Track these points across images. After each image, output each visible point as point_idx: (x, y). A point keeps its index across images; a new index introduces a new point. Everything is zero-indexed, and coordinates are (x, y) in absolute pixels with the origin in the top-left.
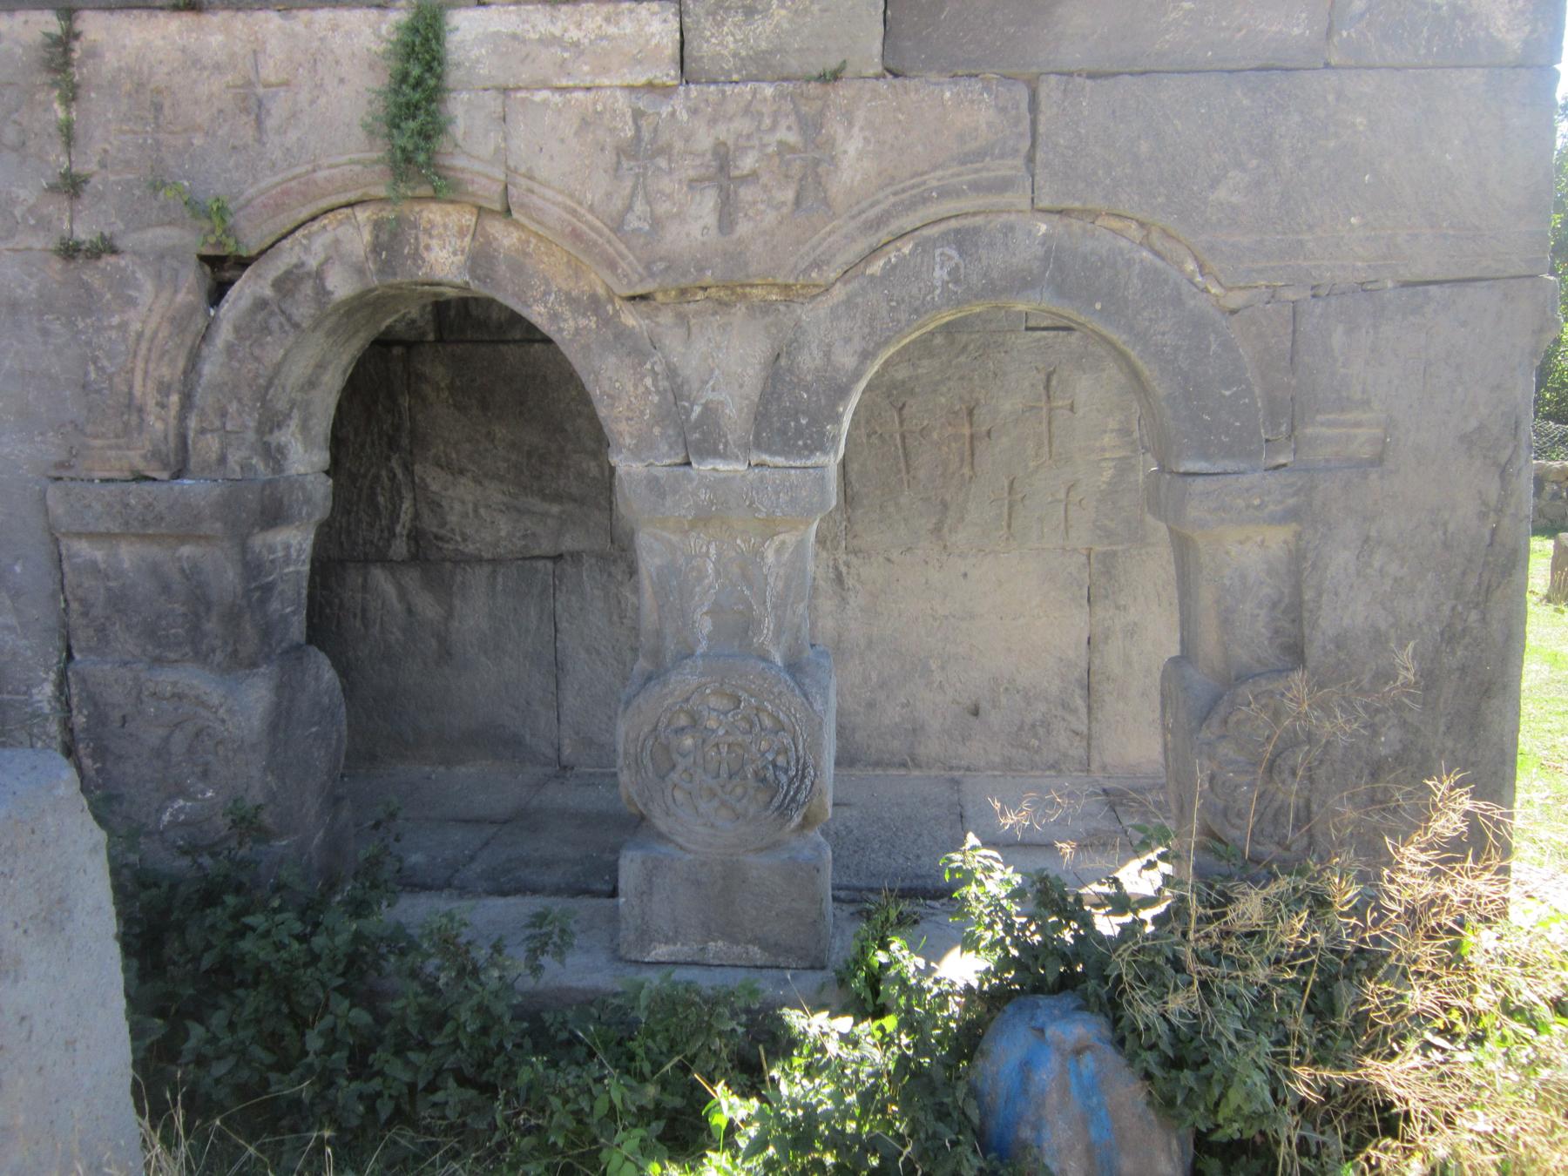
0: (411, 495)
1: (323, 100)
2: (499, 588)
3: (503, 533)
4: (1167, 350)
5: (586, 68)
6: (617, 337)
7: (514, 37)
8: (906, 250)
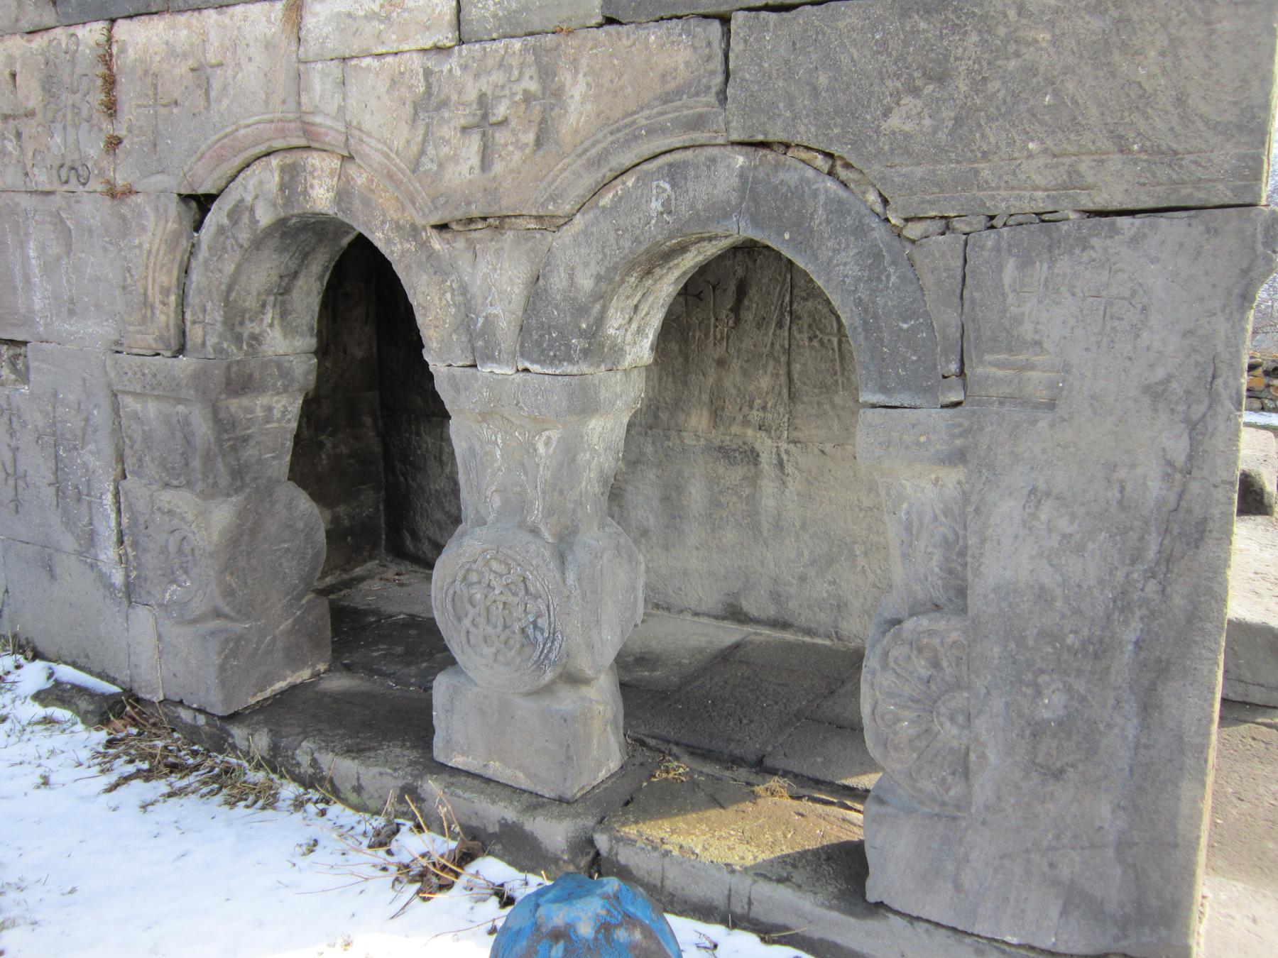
1: (240, 75)
4: (848, 281)
5: (394, 37)
6: (429, 257)
7: (349, 15)
8: (630, 184)
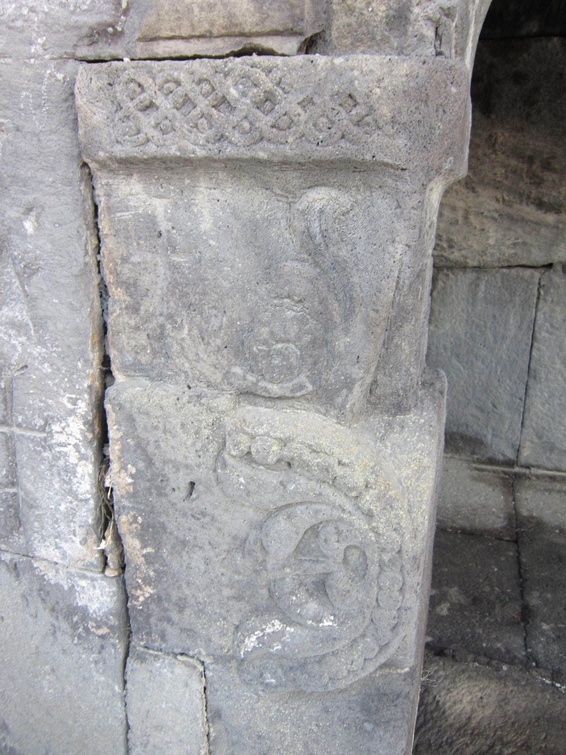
2: (481, 295)
3: (491, 242)
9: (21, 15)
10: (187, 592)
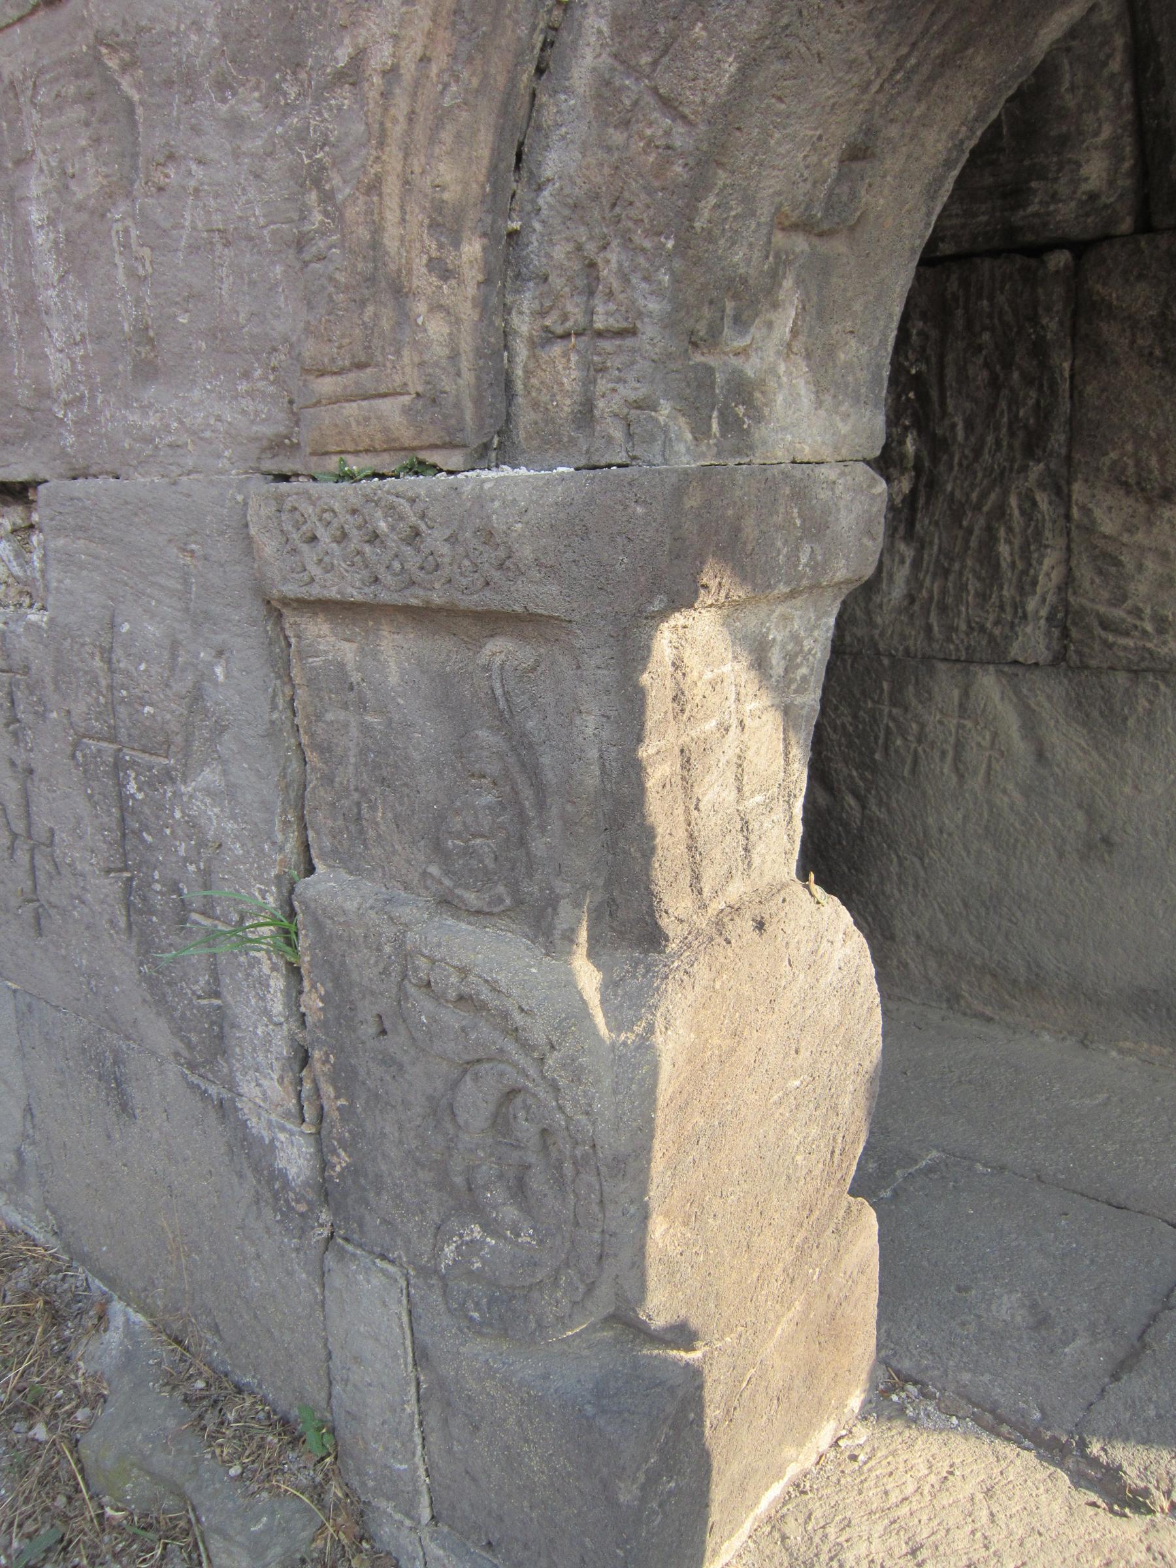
0: (1062, 542)
9: (209, 425)
10: (384, 1168)
